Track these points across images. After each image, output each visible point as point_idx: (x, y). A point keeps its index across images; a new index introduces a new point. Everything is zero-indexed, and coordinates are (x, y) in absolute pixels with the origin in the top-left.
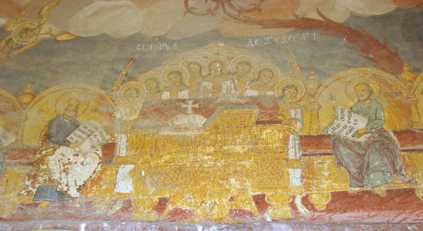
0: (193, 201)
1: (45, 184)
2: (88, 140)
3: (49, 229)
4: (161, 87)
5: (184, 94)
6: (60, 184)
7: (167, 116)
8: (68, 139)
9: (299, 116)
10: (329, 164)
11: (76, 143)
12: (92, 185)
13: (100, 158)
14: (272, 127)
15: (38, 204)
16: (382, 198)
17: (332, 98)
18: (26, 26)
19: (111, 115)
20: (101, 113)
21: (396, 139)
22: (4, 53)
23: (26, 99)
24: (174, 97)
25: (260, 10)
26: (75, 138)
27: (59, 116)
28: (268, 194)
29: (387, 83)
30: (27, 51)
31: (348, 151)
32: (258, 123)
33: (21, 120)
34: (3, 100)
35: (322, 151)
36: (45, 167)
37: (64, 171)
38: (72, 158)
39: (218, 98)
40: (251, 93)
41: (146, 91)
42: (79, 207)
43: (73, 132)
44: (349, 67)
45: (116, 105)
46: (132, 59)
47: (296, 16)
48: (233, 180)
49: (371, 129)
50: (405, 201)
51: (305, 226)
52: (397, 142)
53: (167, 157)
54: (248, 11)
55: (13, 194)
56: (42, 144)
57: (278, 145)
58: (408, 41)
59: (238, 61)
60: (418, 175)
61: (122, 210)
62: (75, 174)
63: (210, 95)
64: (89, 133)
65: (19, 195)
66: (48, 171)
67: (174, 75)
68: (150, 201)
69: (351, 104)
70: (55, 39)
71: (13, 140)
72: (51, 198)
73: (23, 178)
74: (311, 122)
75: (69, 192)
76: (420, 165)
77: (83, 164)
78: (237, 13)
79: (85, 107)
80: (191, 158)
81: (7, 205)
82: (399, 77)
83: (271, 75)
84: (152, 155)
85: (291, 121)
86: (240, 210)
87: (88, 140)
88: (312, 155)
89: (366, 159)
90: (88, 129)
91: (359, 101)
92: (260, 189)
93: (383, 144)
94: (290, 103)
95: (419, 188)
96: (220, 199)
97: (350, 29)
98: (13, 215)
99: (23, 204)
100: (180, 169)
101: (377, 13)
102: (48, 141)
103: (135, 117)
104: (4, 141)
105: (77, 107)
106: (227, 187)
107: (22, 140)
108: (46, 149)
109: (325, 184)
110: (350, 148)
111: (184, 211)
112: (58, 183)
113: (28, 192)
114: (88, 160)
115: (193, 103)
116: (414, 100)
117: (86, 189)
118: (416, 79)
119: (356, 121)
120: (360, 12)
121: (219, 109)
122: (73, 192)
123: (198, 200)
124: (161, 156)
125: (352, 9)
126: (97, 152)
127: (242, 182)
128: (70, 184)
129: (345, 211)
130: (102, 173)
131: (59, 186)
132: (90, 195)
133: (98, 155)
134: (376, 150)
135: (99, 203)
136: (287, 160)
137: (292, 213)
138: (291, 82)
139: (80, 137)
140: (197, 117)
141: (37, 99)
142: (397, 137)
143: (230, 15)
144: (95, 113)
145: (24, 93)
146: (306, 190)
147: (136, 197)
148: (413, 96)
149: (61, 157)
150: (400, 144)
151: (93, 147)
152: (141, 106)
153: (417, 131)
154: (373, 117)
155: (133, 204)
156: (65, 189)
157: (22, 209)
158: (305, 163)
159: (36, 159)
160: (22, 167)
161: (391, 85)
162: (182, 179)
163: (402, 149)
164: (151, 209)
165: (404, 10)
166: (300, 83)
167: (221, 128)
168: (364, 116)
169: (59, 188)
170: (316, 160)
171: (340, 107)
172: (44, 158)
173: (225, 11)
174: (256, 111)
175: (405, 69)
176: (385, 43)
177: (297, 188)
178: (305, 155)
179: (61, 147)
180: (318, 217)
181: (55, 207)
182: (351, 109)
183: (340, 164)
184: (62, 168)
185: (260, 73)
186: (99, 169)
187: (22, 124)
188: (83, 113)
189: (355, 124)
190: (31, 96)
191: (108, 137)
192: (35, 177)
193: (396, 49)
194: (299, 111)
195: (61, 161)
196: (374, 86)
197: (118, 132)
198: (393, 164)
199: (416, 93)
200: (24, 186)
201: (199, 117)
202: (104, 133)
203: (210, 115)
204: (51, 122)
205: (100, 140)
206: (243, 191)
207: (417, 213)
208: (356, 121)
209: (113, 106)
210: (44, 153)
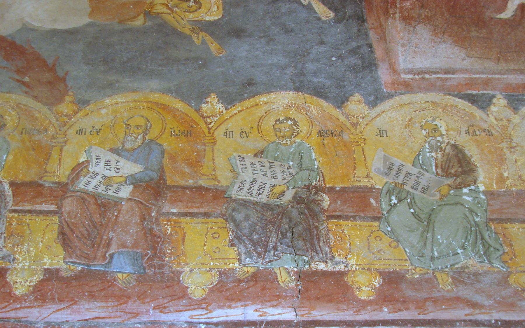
21: (10, 193)
29: (32, 117)
58: (88, 64)
60: (21, 248)
76: (31, 233)
82: (54, 108)
95: (15, 269)
101: (60, 26)
116: (61, 141)
118: (77, 113)
120: (36, 24)
125: (28, 19)
142: (12, 190)
148: (63, 136)
150: (14, 201)
153: (47, 184)
161: (37, 119)
163: (13, 208)
165: (99, 26)
175: (68, 99)
176: (54, 65)
193: (67, 73)
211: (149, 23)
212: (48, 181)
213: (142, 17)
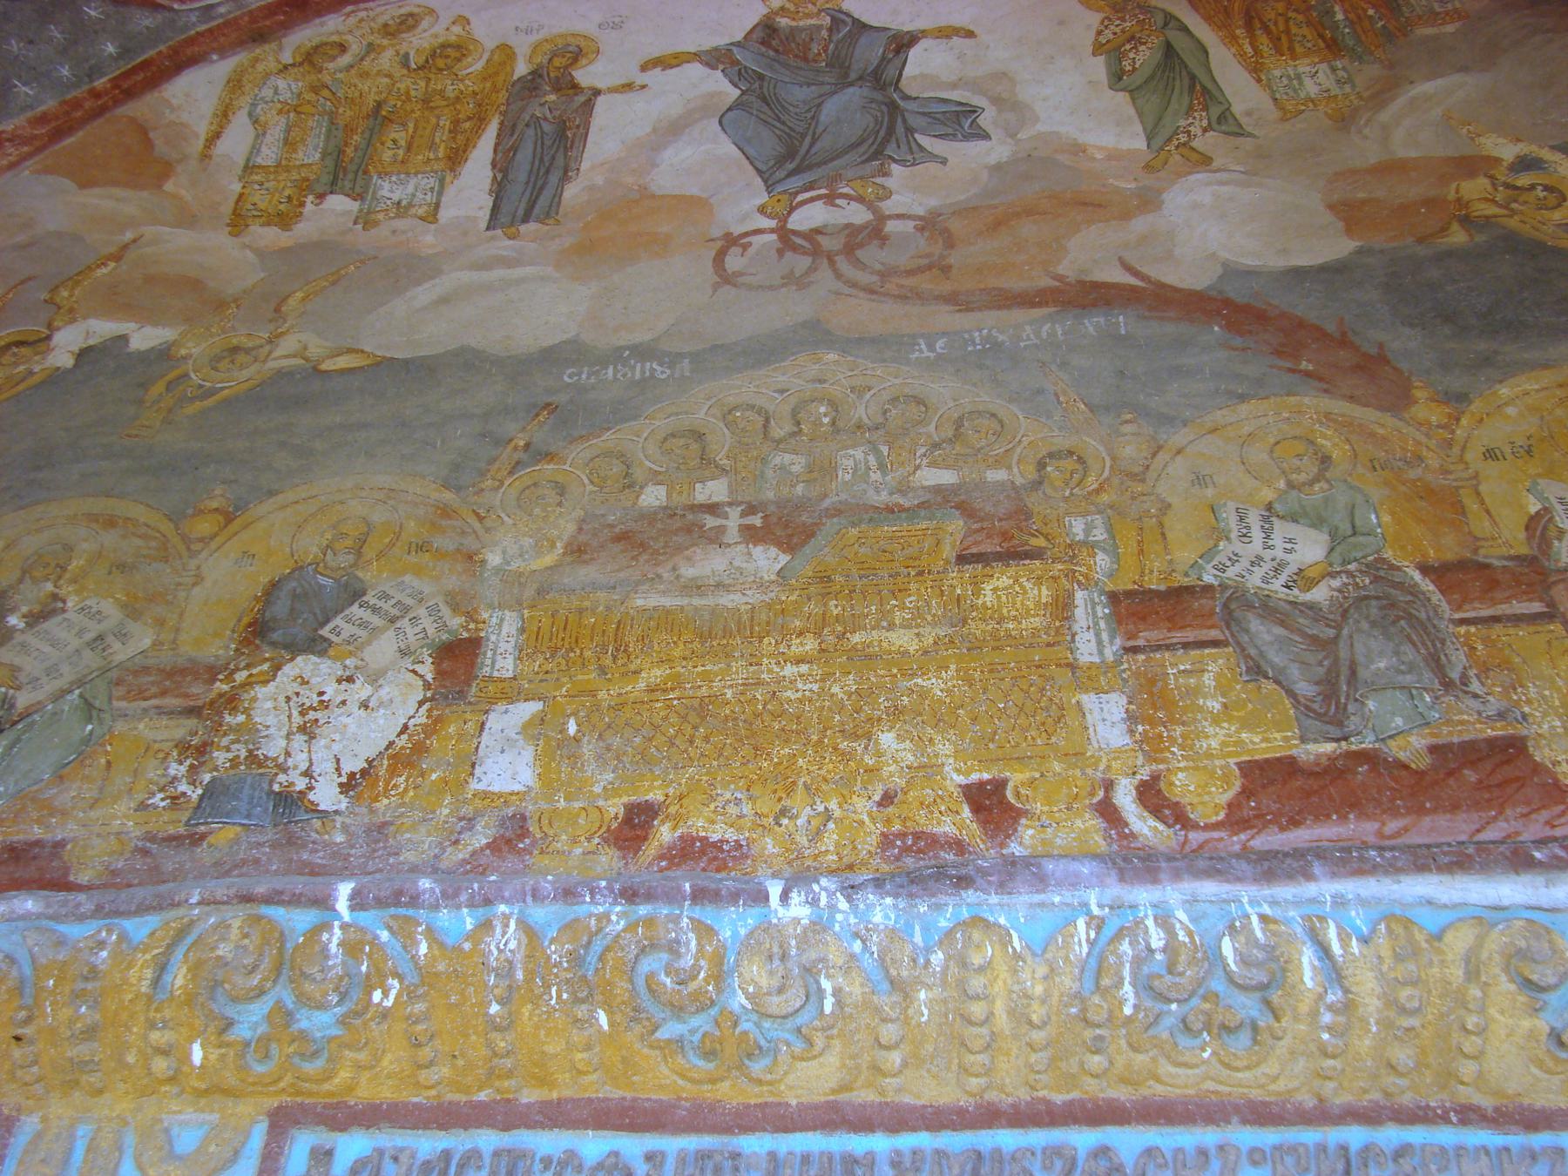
0: (747, 809)
1: (232, 772)
2: (391, 633)
3: (224, 903)
4: (638, 474)
5: (714, 490)
6: (285, 770)
7: (656, 552)
8: (325, 632)
9: (1099, 534)
10: (1218, 677)
11: (349, 643)
12: (393, 772)
13: (427, 686)
14: (1012, 571)
15: (203, 837)
16: (1420, 774)
17: (1200, 480)
18: (235, 341)
19: (471, 558)
20: (440, 555)
21: (1432, 587)
22: (157, 411)
23: (204, 527)
24: (680, 500)
25: (946, 270)
26: (348, 630)
27: (302, 567)
28: (1016, 778)
29: (1372, 435)
30: (227, 402)
31: (1279, 630)
32: (962, 559)
33: (179, 584)
34: (133, 534)
35: (1190, 635)
36: (241, 718)
37: (303, 729)
38: (331, 690)
39: (826, 496)
40: (933, 477)
41: (590, 488)
42: (341, 843)
43: (342, 611)
44: (1243, 398)
45: (488, 530)
46: (549, 405)
47: (1059, 278)
48: (887, 739)
49: (1345, 562)
50: (1498, 777)
51: (1163, 865)
52: (1437, 597)
53: (657, 674)
54: (910, 273)
55: (123, 807)
56: (237, 650)
57: (1036, 622)
58: (1411, 325)
59: (886, 396)
60: (1524, 694)
61: (494, 846)
62: (337, 737)
63: (799, 489)
64: (394, 612)
65: (142, 806)
66: (250, 731)
67: (682, 441)
68: (595, 815)
69: (1268, 494)
70: (315, 369)
71: (147, 642)
72: (248, 816)
73: (161, 755)
74: (1141, 552)
75: (311, 796)
76: (1524, 662)
77: (367, 707)
78: (875, 278)
79: (387, 540)
80: (740, 671)
81: (96, 841)
82: (1407, 416)
83: (995, 425)
84: (603, 670)
85: (1074, 551)
86: (917, 836)
87: (391, 633)
88: (1158, 648)
89: (1343, 653)
90: (393, 601)
91: (1291, 485)
92: (985, 762)
93: (1393, 605)
94: (1066, 499)
95: (1540, 735)
96: (843, 802)
97: (1227, 302)
98: (114, 873)
99: (151, 837)
100: (702, 709)
101: (1303, 260)
102: (257, 642)
103: (548, 560)
104: (117, 646)
105: (362, 541)
106: (869, 761)
107: (174, 641)
108: (248, 667)
109: (1214, 738)
110: (1282, 623)
111: (717, 846)
112: (278, 766)
113: (174, 798)
114: (384, 693)
115: (744, 514)
116: (1465, 475)
117: (374, 785)
118: (1458, 420)
119: (1290, 541)
120: (1250, 262)
121: (831, 525)
122: (326, 795)
123: (767, 805)
124: (637, 672)
125: (1224, 255)
126: (418, 668)
127: (921, 743)
128: (317, 770)
129: (1295, 823)
130: (430, 730)
131: (282, 778)
132: (386, 801)
133: (421, 676)
134: (1373, 624)
135: (413, 828)
136: (1073, 667)
137: (1107, 837)
138: (1062, 442)
139: (363, 624)
140: (758, 551)
141: (238, 522)
142: (1432, 581)
143: (854, 285)
144: (420, 553)
145: (201, 512)
146: (1150, 758)
147: (544, 805)
148: (1461, 466)
149: (296, 687)
150: (1449, 603)
151: (404, 653)
152: (571, 528)
153: (1496, 563)
154: (1345, 527)
155: (533, 828)
156: (301, 784)
157: (145, 852)
158: (1137, 674)
159: (213, 695)
160: (164, 721)
161: (1385, 439)
162: (707, 739)
163: (1457, 616)
164: (596, 841)
165: (1382, 251)
166: (1092, 444)
167: (839, 578)
168: (1313, 526)
169: (281, 784)
170: (1175, 666)
171: (1231, 505)
172: (240, 691)
173: (838, 275)
174: (956, 526)
175: (1419, 394)
176: (1344, 334)
177: (1118, 753)
178: (1135, 650)
179: (299, 658)
180: (1201, 847)
181: (259, 845)
182: (1269, 507)
183: (1256, 671)
184: (297, 719)
185: (959, 424)
186: (421, 718)
187: (182, 595)
188: (380, 555)
189: (1290, 551)
190: (221, 518)
191: (456, 622)
192: (203, 750)
193: (1381, 346)
194: (1098, 520)
195: (295, 698)
196: (1328, 441)
197: (491, 606)
198: (1436, 663)
199: (1469, 456)
200: (163, 781)
201: (765, 551)
202: (446, 611)
203: (804, 543)
204: (274, 586)
205: (431, 631)
206: (927, 771)
207: (1545, 815)
208: (1290, 541)
209: (481, 532)
210: (241, 676)
211: (1480, 238)
212: (1492, 554)
213: (1455, 226)
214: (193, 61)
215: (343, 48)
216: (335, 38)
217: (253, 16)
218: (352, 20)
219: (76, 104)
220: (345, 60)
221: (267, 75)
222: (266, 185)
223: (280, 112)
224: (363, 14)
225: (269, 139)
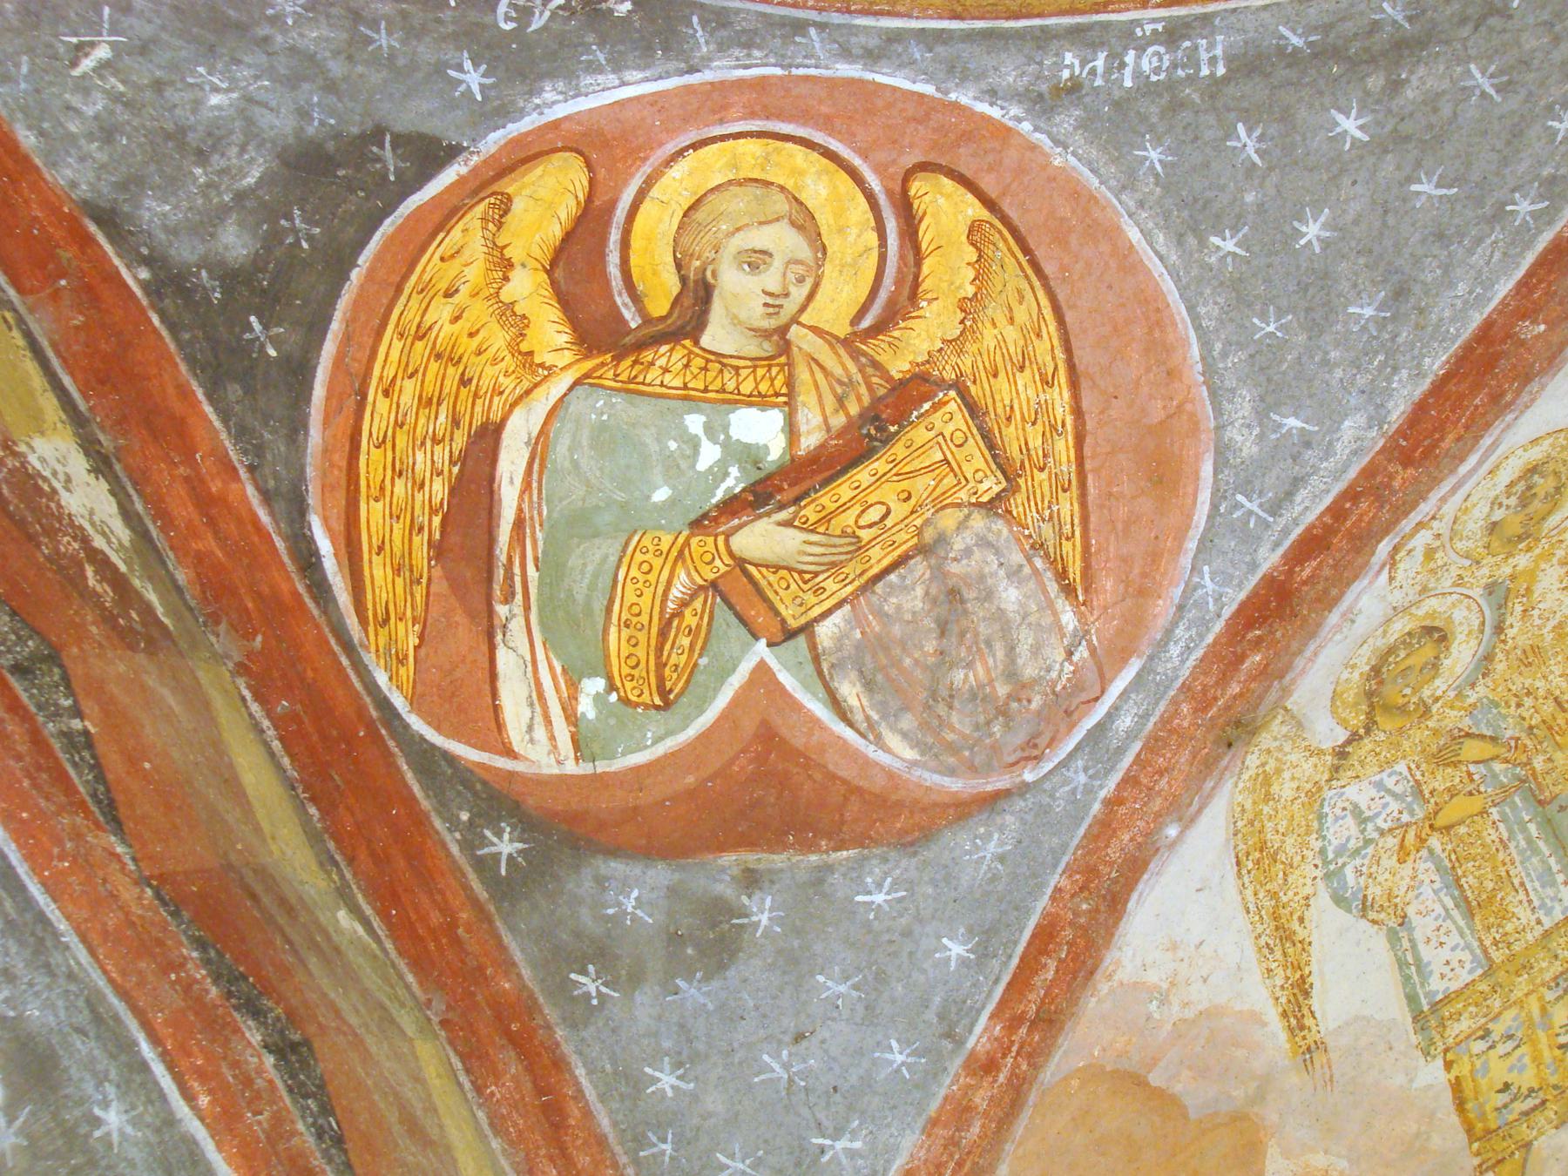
214: (1135, 868)
215: (1437, 635)
216: (1400, 627)
217: (1198, 696)
218: (1409, 567)
219: (960, 1111)
220: (1461, 655)
221: (1313, 796)
222: (1498, 1029)
223: (1403, 854)
224: (1423, 539)
225: (1422, 927)
